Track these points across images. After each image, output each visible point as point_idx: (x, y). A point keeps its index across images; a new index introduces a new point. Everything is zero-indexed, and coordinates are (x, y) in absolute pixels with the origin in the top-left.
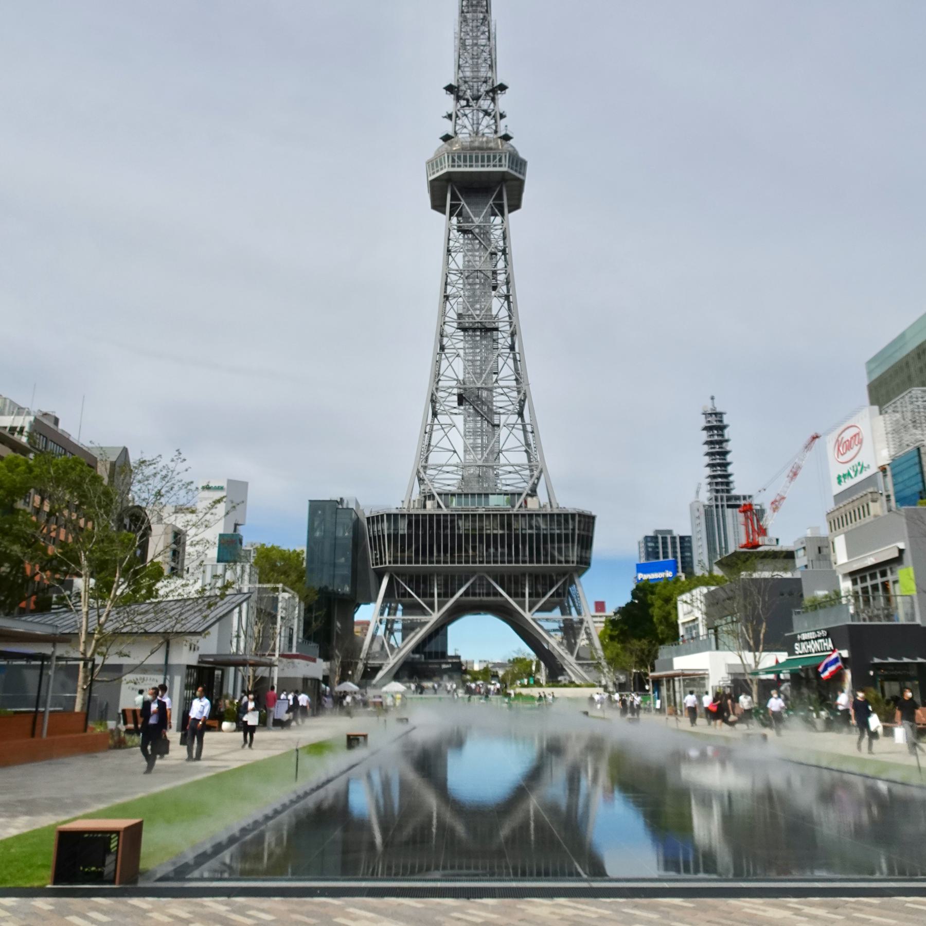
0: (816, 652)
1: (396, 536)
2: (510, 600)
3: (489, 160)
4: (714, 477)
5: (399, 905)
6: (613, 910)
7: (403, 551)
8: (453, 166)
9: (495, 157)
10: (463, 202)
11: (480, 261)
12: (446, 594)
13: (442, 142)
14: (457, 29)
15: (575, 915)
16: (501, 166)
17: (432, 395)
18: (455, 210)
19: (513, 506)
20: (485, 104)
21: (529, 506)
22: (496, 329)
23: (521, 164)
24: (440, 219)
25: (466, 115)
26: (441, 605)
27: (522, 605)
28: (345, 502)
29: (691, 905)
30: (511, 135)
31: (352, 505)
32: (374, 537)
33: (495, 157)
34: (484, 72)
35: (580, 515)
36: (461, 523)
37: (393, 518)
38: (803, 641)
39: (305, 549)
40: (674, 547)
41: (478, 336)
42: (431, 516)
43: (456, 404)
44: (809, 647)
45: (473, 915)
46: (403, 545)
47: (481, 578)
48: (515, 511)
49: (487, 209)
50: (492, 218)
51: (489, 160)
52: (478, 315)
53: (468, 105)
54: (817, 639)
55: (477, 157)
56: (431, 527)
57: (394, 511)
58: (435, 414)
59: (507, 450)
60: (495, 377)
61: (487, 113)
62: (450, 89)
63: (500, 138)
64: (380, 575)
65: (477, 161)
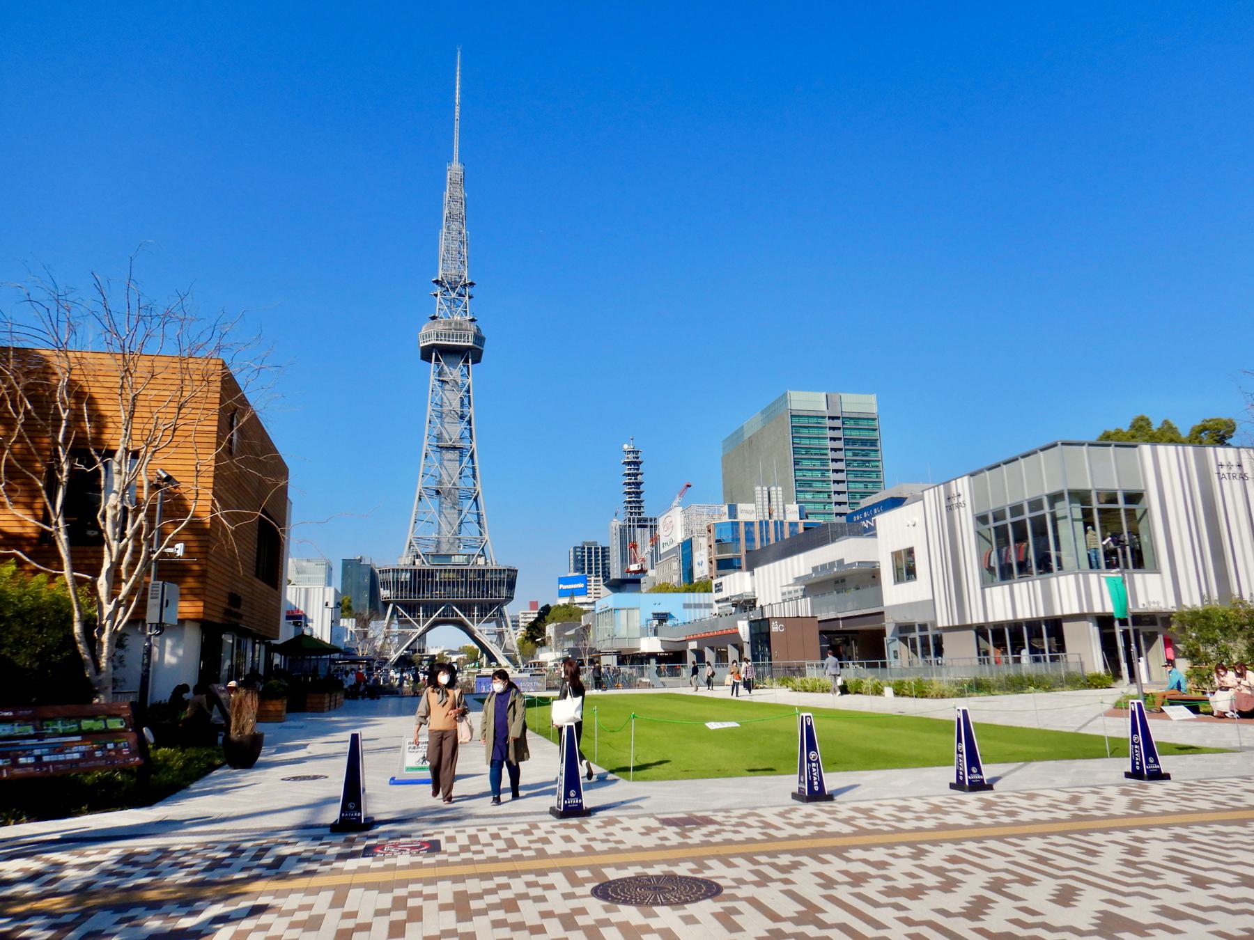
1: (398, 581)
2: (465, 619)
4: (630, 502)
9: (465, 336)
10: (443, 363)
12: (427, 616)
26: (425, 622)
27: (472, 621)
33: (465, 336)
36: (438, 574)
40: (597, 556)
42: (420, 570)
46: (402, 587)
47: (448, 606)
48: (469, 567)
51: (461, 338)
55: (453, 335)
64: (386, 604)
65: (453, 338)
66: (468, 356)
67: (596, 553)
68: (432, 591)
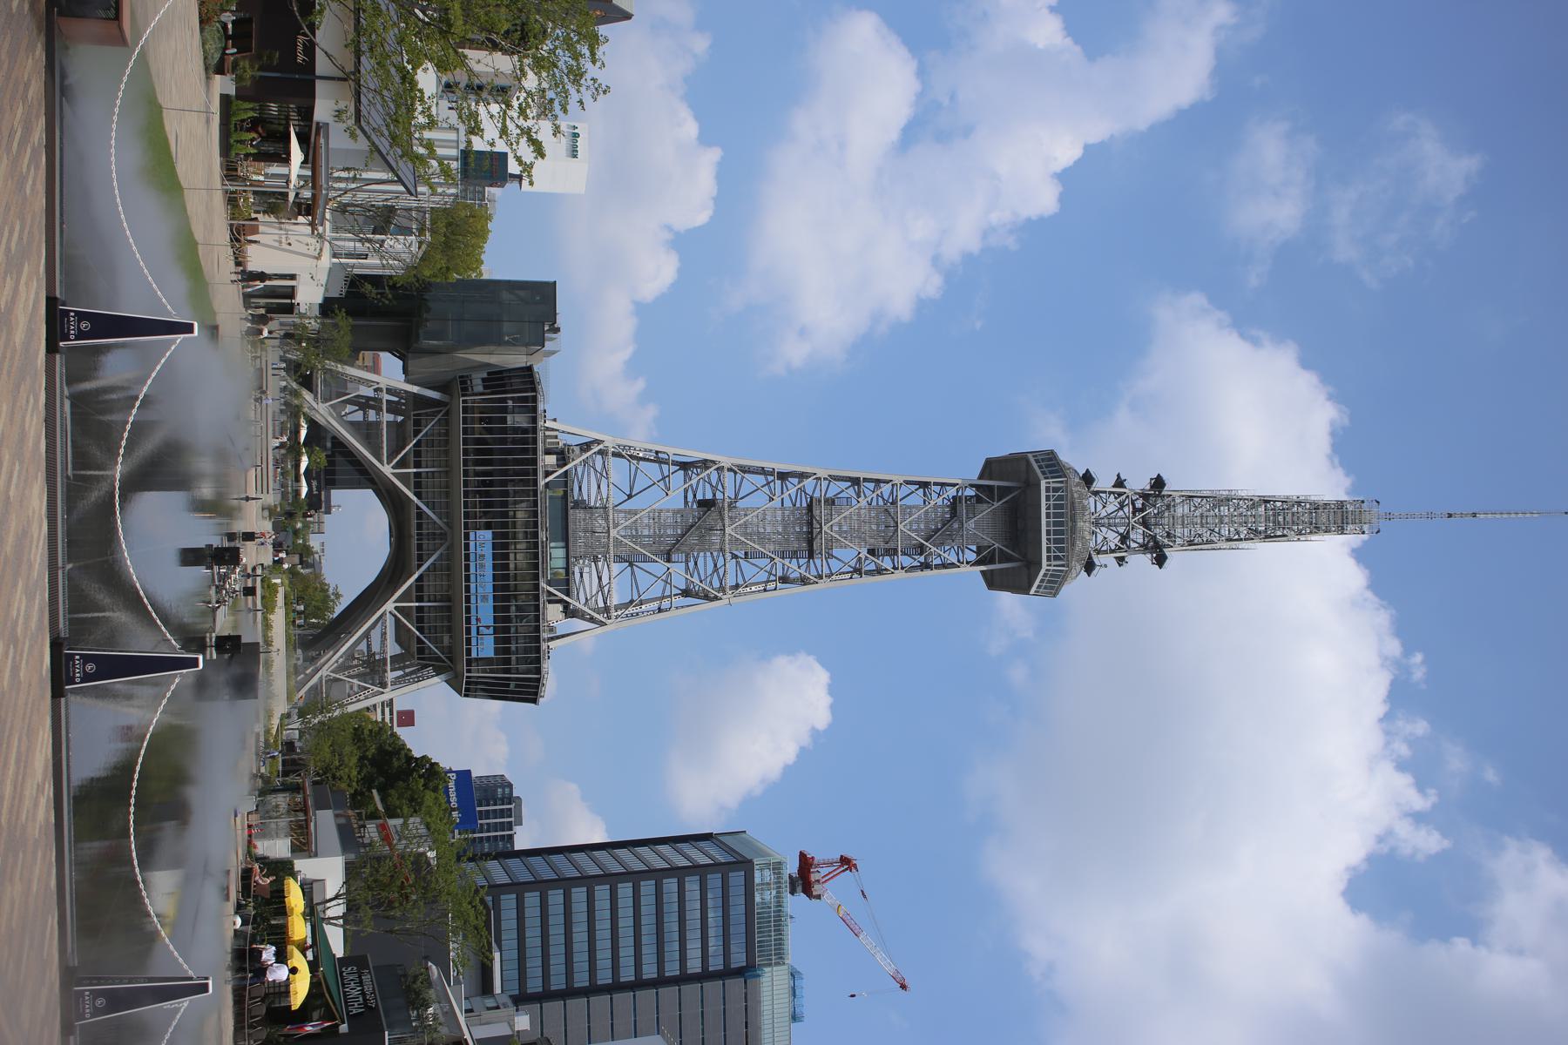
0: (344, 993)
3: (1056, 541)
5: (40, 339)
6: (37, 581)
7: (481, 420)
8: (1048, 489)
10: (996, 505)
11: (908, 529)
13: (1082, 472)
14: (1243, 494)
15: (32, 536)
16: (1049, 559)
18: (984, 493)
19: (549, 583)
20: (1138, 535)
21: (550, 607)
23: (1052, 588)
24: (973, 472)
25: (1122, 507)
28: (554, 336)
29: (44, 673)
31: (548, 345)
32: (502, 379)
33: (1061, 550)
35: (538, 680)
37: (530, 405)
38: (360, 977)
39: (486, 276)
41: (801, 528)
42: (534, 462)
43: (700, 497)
44: (352, 985)
45: (32, 420)
46: (490, 421)
48: (543, 584)
49: (987, 540)
50: (974, 548)
51: (1056, 541)
52: (829, 528)
53: (1135, 511)
54: (363, 994)
55: (1061, 524)
56: (517, 462)
57: (541, 407)
58: (684, 466)
59: (633, 573)
61: (1124, 538)
62: (1158, 483)
63: (1090, 557)
67: (502, 826)
68: (481, 494)
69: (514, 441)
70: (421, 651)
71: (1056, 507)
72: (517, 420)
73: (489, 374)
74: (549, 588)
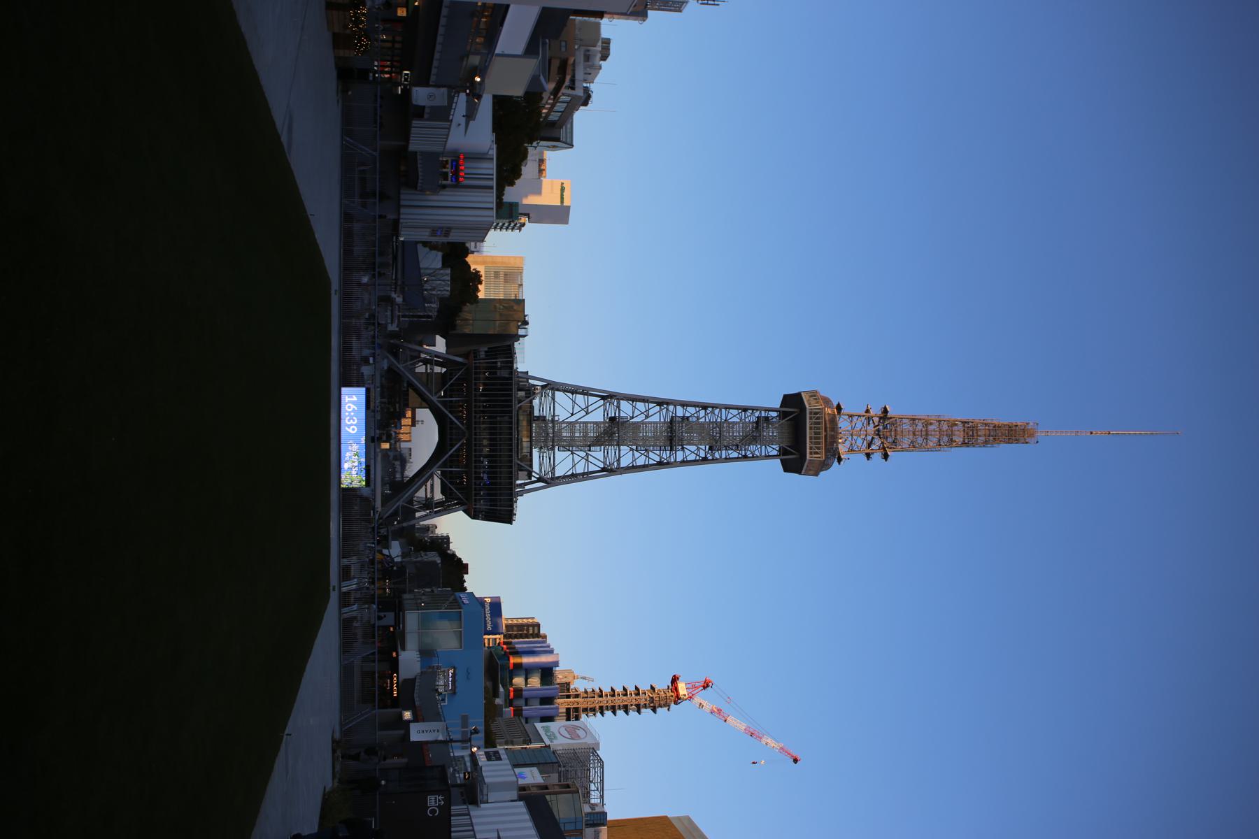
8: (811, 413)
13: (835, 404)
16: (811, 453)
17: (615, 396)
19: (521, 460)
22: (671, 450)
24: (777, 404)
27: (444, 465)
30: (842, 463)
33: (819, 448)
34: (906, 442)
35: (512, 510)
36: (506, 419)
42: (511, 395)
43: (609, 416)
48: (515, 460)
51: (815, 443)
55: (819, 433)
56: (503, 395)
57: (515, 367)
60: (634, 447)
62: (885, 411)
64: (466, 356)
66: (792, 454)
69: (501, 384)
70: (451, 494)
71: (815, 423)
72: (504, 373)
73: (489, 348)
74: (519, 462)
